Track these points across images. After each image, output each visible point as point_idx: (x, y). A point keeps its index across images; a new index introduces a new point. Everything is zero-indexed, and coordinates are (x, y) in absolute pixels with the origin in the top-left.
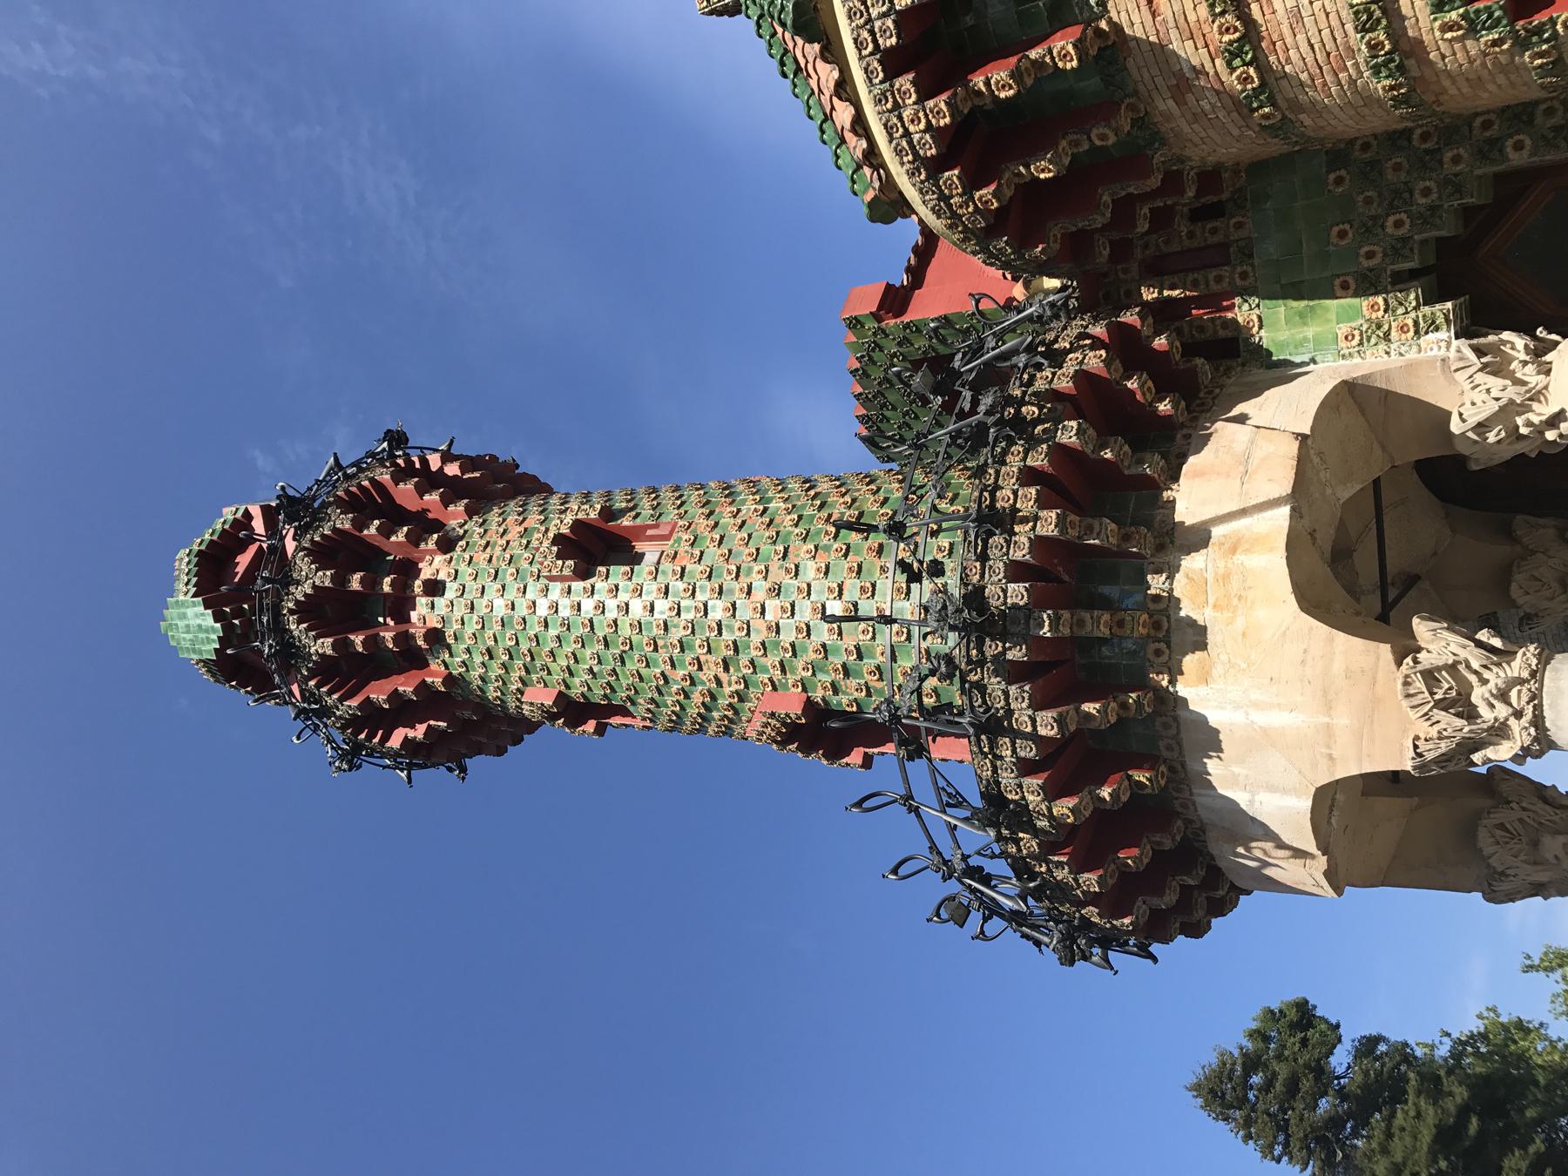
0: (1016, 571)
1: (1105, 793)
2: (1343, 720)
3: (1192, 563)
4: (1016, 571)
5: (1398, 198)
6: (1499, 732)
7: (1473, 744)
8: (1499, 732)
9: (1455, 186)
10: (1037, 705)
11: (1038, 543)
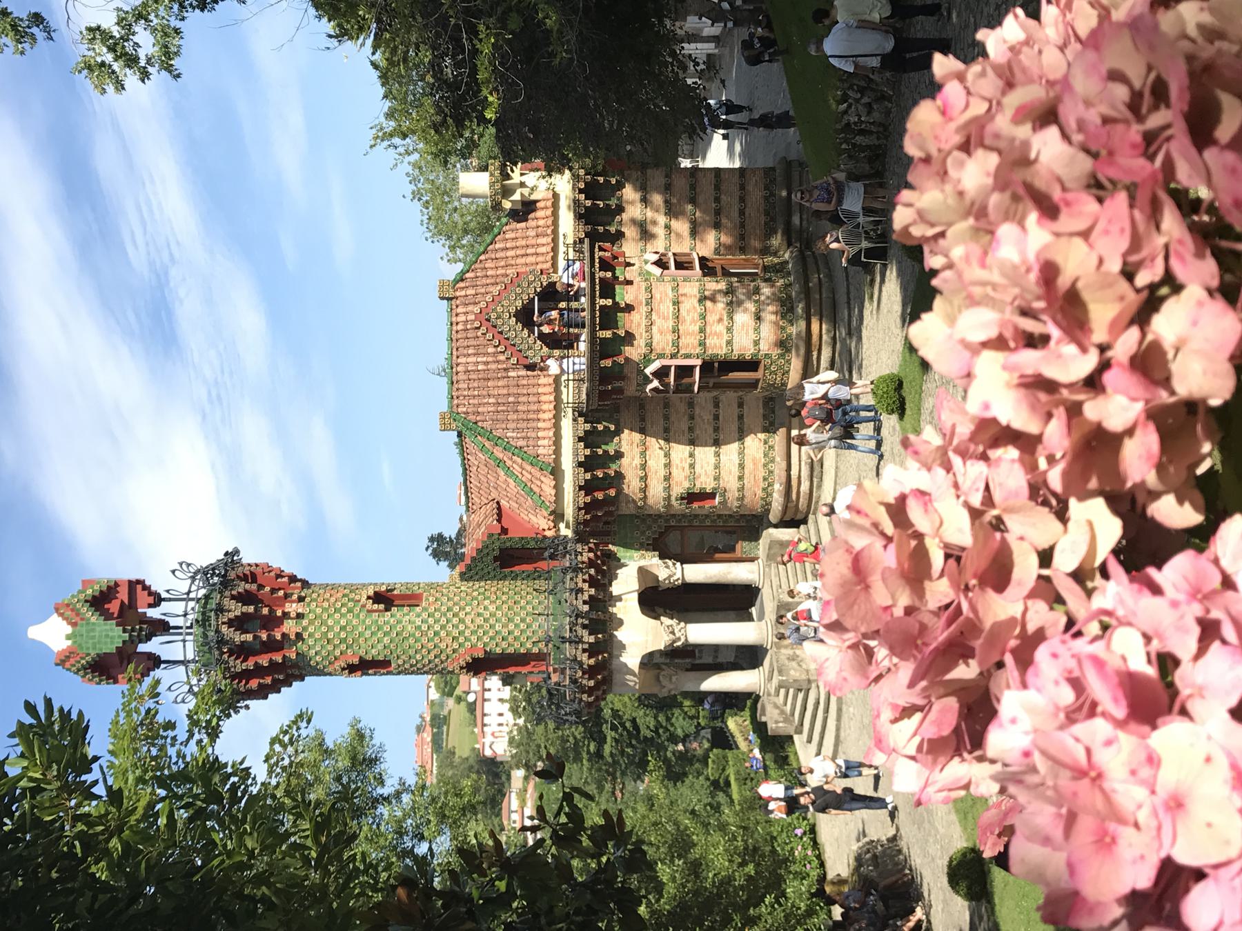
0: (585, 602)
1: (600, 657)
3: (618, 604)
4: (585, 602)
5: (649, 528)
6: (679, 639)
7: (674, 642)
8: (679, 639)
9: (659, 527)
10: (590, 634)
11: (590, 596)
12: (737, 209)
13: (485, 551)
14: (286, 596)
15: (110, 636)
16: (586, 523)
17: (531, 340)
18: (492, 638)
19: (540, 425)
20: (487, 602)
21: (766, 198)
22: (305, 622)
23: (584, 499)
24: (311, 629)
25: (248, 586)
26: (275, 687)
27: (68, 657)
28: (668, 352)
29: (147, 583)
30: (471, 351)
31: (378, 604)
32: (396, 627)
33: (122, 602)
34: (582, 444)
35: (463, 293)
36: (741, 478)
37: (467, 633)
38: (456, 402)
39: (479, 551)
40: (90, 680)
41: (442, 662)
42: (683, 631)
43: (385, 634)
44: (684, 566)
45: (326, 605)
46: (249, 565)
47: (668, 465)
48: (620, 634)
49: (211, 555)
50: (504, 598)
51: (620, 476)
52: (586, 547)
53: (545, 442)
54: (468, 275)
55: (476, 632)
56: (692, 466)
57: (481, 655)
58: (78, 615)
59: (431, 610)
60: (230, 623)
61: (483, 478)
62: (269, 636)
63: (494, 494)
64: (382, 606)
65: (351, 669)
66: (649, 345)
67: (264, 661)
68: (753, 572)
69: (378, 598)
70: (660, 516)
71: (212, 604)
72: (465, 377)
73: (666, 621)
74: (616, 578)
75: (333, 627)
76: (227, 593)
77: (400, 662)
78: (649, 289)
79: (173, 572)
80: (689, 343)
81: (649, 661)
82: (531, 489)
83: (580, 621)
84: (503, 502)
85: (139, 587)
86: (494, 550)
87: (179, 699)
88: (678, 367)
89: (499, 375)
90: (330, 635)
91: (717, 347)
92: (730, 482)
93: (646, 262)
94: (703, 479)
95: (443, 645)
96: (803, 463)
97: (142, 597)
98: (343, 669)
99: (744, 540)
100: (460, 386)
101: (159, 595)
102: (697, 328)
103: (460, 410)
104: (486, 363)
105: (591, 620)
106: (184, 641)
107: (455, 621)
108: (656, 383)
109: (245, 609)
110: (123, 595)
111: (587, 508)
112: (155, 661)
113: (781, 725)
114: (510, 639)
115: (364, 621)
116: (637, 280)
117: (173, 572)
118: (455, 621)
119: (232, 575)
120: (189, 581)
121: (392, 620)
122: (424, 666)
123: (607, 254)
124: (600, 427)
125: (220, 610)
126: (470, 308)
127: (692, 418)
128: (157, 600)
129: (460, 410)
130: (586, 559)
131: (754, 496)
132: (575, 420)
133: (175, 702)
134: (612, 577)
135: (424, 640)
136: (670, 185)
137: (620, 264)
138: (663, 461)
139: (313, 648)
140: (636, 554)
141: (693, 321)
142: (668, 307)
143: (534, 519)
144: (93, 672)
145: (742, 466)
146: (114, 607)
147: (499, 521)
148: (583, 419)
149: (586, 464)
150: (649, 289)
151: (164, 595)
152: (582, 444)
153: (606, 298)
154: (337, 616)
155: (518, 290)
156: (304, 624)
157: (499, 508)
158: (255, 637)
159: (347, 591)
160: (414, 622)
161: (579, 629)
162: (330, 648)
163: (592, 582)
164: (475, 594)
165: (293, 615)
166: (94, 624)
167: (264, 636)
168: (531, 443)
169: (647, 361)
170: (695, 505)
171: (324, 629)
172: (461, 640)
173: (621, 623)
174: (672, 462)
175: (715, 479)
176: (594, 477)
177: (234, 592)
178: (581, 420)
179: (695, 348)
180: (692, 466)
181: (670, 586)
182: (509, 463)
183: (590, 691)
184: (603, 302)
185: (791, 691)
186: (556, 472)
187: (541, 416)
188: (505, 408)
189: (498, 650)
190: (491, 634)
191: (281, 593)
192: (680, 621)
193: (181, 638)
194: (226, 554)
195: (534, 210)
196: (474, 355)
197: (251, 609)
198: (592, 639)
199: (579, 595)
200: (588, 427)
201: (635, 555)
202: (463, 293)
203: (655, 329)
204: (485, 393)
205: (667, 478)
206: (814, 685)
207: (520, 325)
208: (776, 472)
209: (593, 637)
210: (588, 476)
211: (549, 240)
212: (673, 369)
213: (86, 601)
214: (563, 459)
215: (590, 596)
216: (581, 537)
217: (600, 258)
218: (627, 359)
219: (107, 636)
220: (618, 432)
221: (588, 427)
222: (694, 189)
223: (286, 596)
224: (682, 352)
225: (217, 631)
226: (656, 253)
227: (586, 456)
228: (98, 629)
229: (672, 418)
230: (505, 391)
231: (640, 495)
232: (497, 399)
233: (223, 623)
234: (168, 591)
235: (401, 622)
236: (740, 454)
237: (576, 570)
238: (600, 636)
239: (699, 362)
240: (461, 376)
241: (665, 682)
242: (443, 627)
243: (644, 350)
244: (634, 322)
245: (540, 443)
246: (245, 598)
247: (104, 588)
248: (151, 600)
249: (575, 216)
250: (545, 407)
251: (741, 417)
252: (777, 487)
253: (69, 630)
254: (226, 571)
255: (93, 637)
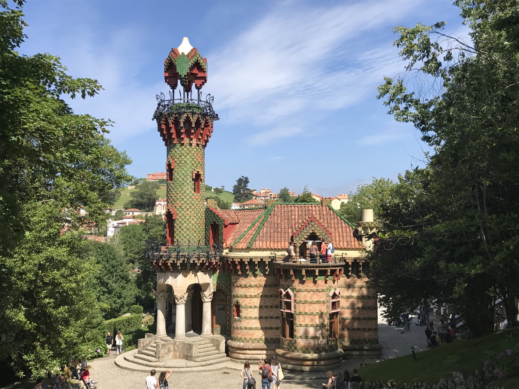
0: (194, 261)
2: (179, 289)
4: (194, 261)
5: (226, 287)
7: (177, 299)
8: (178, 301)
11: (197, 263)
12: (360, 327)
13: (217, 218)
14: (199, 139)
15: (183, 70)
16: (227, 261)
17: (303, 239)
18: (180, 222)
19: (268, 242)
20: (195, 220)
21: (365, 340)
22: (188, 147)
23: (237, 261)
24: (185, 149)
25: (203, 124)
26: (162, 135)
27: (175, 53)
28: (297, 298)
29: (205, 84)
30: (300, 212)
31: (196, 176)
32: (186, 183)
33: (197, 74)
34: (260, 260)
35: (324, 209)
36: (246, 328)
37: (183, 212)
38: (279, 206)
39: (218, 216)
40: (166, 62)
41: (171, 202)
42: (182, 303)
43: (183, 179)
44: (210, 302)
45: (195, 155)
46: (212, 124)
47: (251, 297)
48: (180, 276)
49: (216, 108)
50: (197, 227)
51: (247, 276)
52: (218, 261)
53: (261, 245)
54: (331, 211)
55: (183, 216)
56: (251, 307)
57: (174, 218)
58: (192, 57)
59: (193, 197)
60: (188, 118)
61: (248, 217)
62: (183, 133)
63: (241, 221)
64: (194, 177)
65: (169, 165)
66: (300, 291)
67: (173, 131)
68: (207, 332)
69: (198, 176)
70: (231, 292)
71: (195, 110)
72: (289, 210)
73: (186, 296)
74: (205, 274)
75: (186, 158)
76: (200, 116)
77: (172, 185)
78: (323, 291)
79: (209, 94)
80: (301, 308)
81: (170, 289)
82: (242, 238)
83: (186, 259)
84: (238, 225)
85: (204, 81)
86: (218, 222)
87: (158, 97)
88: (291, 302)
89: (290, 225)
90: (183, 157)
91: (299, 320)
92: (244, 324)
93: (335, 289)
94: (245, 312)
95: (178, 202)
96: (252, 356)
97: (198, 82)
98: (169, 162)
99: (221, 328)
100: (286, 208)
101: (201, 89)
102: (307, 311)
103: (276, 208)
104: (295, 219)
105: (187, 264)
106: (181, 99)
107: (188, 207)
108: (284, 293)
109: (193, 123)
110: (200, 75)
111: (233, 262)
112: (174, 87)
113: (142, 344)
114: (180, 230)
115: (188, 170)
116: (327, 285)
117: (209, 94)
118: (188, 207)
119: (208, 118)
120: (205, 101)
121: (189, 181)
122: (170, 194)
123: (338, 273)
124: (267, 268)
125: (193, 113)
126: (318, 212)
127: (271, 307)
128: (198, 88)
129: (276, 208)
130: (212, 261)
131: (237, 334)
132: (270, 257)
133: (157, 95)
134: (205, 272)
135: (180, 195)
136: (370, 298)
137: (334, 278)
138: (253, 294)
139: (178, 150)
140: (215, 282)
141: (310, 310)
142: (316, 299)
143: (231, 238)
144: (169, 63)
145: (251, 329)
146: (195, 71)
147: (230, 224)
148: (270, 261)
149: (251, 262)
150: (323, 291)
151: (200, 90)
152: (260, 260)
153: (319, 272)
154: (191, 159)
155: (324, 234)
156: (187, 146)
157: (236, 224)
158: (182, 127)
159: (201, 163)
160: (187, 190)
161: (183, 259)
162: (178, 157)
163: (203, 264)
164: (199, 215)
165: (191, 142)
166: (188, 64)
167: (182, 131)
168: (261, 238)
169: (293, 290)
170: (234, 308)
171: (185, 154)
172: (180, 210)
173: (185, 276)
174: (252, 299)
175: (245, 317)
176: (246, 265)
177: (200, 119)
178: (270, 260)
179: (298, 310)
180: (251, 307)
181: (202, 296)
182: (253, 229)
183: (157, 263)
184: (317, 271)
185: (155, 349)
186: (248, 249)
187: (272, 243)
188: (276, 227)
189: (175, 225)
190: (182, 222)
191: (200, 137)
192: (186, 301)
193: (182, 98)
194: (217, 115)
195: (358, 240)
196: (299, 214)
197: (193, 126)
198: (178, 264)
199: (197, 259)
200: (267, 263)
201: (215, 282)
202: (324, 209)
203: (306, 293)
204: (282, 218)
205: (246, 296)
206: (157, 360)
207: (309, 234)
208: (248, 344)
209: (179, 265)
210: (246, 263)
211: (345, 247)
212: (290, 300)
213: (197, 60)
214: (254, 252)
215: (197, 263)
216: (222, 258)
217: (336, 269)
218: (293, 281)
219: (183, 69)
220: (265, 275)
221: (267, 263)
222: (368, 309)
223: (199, 139)
224: (297, 305)
225: (184, 113)
226: (339, 293)
227: (254, 262)
228: (186, 65)
229: (271, 298)
230: (283, 227)
231: (239, 285)
232: (280, 224)
233: (188, 115)
234: (201, 93)
235: (188, 185)
236: (256, 328)
237: (208, 257)
238: (180, 268)
239: (293, 312)
240: (290, 209)
241: (161, 294)
242: (185, 202)
243: (297, 288)
244: (309, 284)
245: (261, 242)
246: (198, 123)
247: (203, 67)
248: (198, 85)
249: (355, 258)
250: (276, 244)
251: (271, 328)
252: (242, 344)
253: (186, 54)
254: (209, 115)
255: (182, 63)
